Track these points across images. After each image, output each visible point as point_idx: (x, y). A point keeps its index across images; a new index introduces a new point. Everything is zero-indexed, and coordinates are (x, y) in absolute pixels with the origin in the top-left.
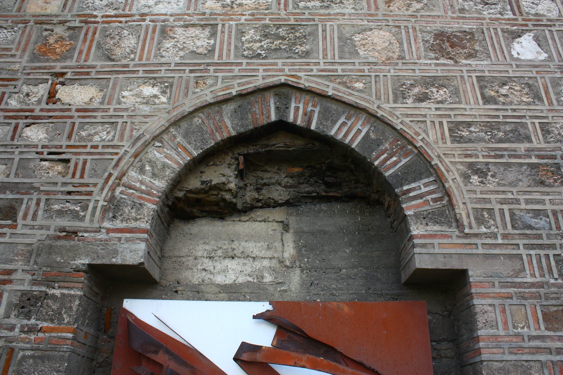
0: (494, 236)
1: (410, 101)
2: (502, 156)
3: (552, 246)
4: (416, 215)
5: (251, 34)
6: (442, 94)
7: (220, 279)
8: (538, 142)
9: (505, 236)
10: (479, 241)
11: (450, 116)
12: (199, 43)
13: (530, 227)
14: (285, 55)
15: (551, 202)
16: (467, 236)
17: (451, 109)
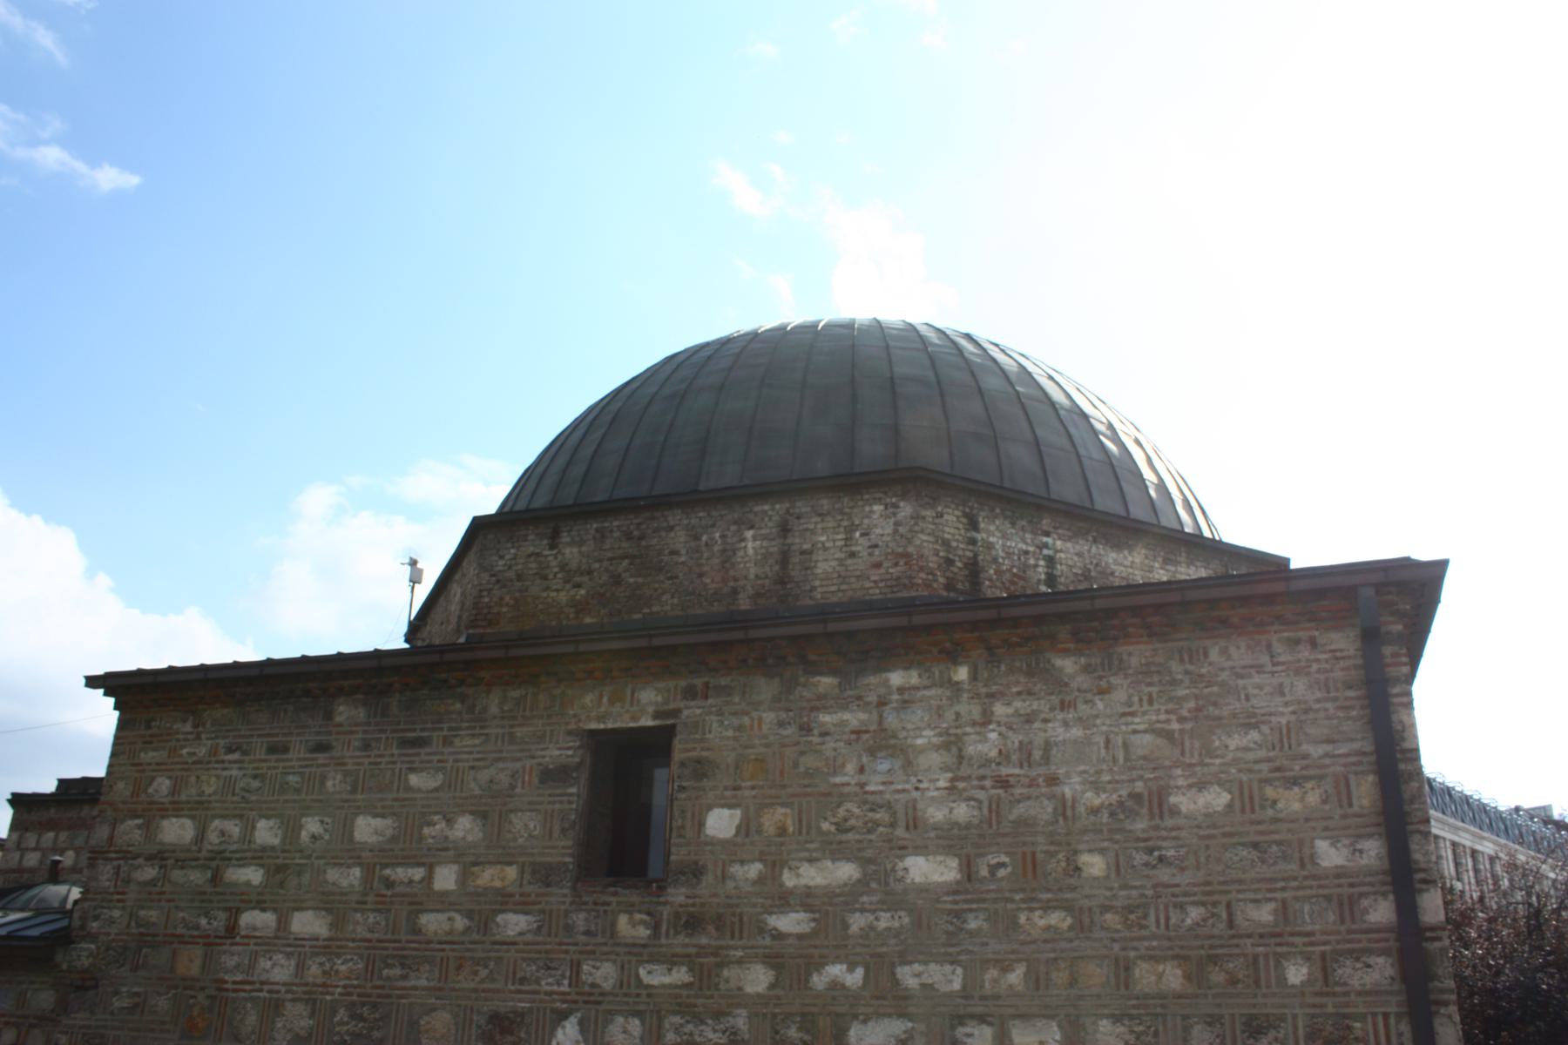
5: (342, 1014)
12: (303, 1023)
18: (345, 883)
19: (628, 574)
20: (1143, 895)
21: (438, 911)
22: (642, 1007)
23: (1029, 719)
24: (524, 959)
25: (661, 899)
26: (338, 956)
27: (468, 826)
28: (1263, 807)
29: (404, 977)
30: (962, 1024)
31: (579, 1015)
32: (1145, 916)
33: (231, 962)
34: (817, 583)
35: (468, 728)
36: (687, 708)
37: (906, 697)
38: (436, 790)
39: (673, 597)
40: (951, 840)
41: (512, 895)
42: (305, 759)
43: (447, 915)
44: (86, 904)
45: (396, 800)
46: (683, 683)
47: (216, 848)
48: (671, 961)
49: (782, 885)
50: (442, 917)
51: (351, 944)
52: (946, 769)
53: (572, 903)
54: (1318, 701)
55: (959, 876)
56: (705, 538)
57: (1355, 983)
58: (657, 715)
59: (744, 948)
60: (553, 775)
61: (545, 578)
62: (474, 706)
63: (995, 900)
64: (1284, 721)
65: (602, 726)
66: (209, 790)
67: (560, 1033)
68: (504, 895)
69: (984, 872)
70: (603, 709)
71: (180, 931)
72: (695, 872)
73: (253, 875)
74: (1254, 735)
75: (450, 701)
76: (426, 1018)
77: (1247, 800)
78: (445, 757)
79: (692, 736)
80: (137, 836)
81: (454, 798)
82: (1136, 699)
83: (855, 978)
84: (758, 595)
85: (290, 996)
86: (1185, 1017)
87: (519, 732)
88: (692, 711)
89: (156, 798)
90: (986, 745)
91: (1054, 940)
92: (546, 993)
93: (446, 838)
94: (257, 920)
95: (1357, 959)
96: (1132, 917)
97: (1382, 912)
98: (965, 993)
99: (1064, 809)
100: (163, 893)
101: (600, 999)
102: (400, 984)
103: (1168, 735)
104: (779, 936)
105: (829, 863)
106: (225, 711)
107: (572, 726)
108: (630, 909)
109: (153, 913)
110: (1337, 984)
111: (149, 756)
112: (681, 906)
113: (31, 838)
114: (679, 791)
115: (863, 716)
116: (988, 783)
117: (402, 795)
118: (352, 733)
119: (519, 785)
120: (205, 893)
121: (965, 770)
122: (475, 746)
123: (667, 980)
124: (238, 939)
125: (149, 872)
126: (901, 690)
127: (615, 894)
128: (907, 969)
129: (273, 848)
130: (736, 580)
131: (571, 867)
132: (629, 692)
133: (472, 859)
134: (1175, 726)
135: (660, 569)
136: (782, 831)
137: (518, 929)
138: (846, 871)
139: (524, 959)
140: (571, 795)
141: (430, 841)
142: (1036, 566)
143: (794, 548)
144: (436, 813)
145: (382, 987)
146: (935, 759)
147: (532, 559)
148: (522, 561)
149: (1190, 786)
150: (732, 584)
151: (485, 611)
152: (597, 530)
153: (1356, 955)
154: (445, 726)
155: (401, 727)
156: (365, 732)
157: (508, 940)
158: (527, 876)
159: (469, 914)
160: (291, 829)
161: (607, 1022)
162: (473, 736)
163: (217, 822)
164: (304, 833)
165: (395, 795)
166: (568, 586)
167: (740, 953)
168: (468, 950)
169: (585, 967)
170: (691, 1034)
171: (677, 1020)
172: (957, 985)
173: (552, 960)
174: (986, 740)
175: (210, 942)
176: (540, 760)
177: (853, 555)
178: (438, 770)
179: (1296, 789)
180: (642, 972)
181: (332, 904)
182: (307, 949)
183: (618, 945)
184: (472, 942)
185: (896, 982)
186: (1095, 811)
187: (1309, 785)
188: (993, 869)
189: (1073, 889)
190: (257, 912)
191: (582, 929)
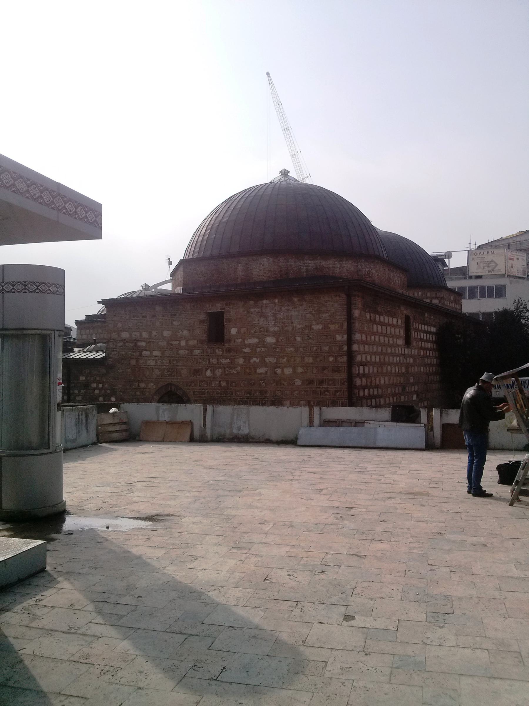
6: (193, 385)
18: (163, 345)
20: (307, 345)
22: (221, 367)
23: (288, 310)
28: (328, 328)
30: (276, 368)
32: (307, 349)
33: (142, 362)
34: (253, 277)
37: (266, 305)
38: (179, 325)
40: (275, 334)
46: (225, 302)
47: (135, 338)
48: (226, 358)
49: (245, 343)
52: (273, 320)
54: (339, 308)
55: (276, 341)
56: (230, 266)
57: (340, 361)
59: (239, 355)
60: (202, 322)
63: (282, 346)
64: (333, 311)
66: (131, 326)
69: (280, 340)
71: (130, 356)
72: (229, 341)
73: (143, 344)
74: (327, 314)
77: (325, 327)
82: (307, 307)
83: (258, 360)
84: (242, 279)
86: (312, 367)
88: (227, 308)
90: (280, 316)
91: (291, 353)
93: (182, 335)
95: (341, 357)
96: (305, 349)
97: (345, 348)
98: (276, 363)
99: (293, 328)
103: (312, 314)
104: (245, 353)
105: (253, 339)
107: (205, 312)
110: (337, 361)
113: (83, 332)
115: (258, 309)
116: (281, 323)
121: (277, 321)
125: (121, 344)
126: (266, 304)
128: (266, 358)
129: (147, 338)
130: (237, 276)
134: (314, 312)
136: (245, 333)
138: (256, 340)
142: (303, 268)
143: (249, 268)
146: (271, 318)
149: (316, 324)
150: (237, 277)
153: (341, 356)
158: (198, 342)
159: (188, 350)
163: (134, 333)
164: (153, 335)
167: (238, 356)
170: (230, 371)
171: (228, 369)
172: (275, 361)
174: (280, 314)
177: (261, 270)
178: (179, 321)
179: (334, 325)
185: (265, 361)
186: (299, 329)
187: (336, 324)
188: (281, 340)
189: (295, 343)
191: (210, 352)
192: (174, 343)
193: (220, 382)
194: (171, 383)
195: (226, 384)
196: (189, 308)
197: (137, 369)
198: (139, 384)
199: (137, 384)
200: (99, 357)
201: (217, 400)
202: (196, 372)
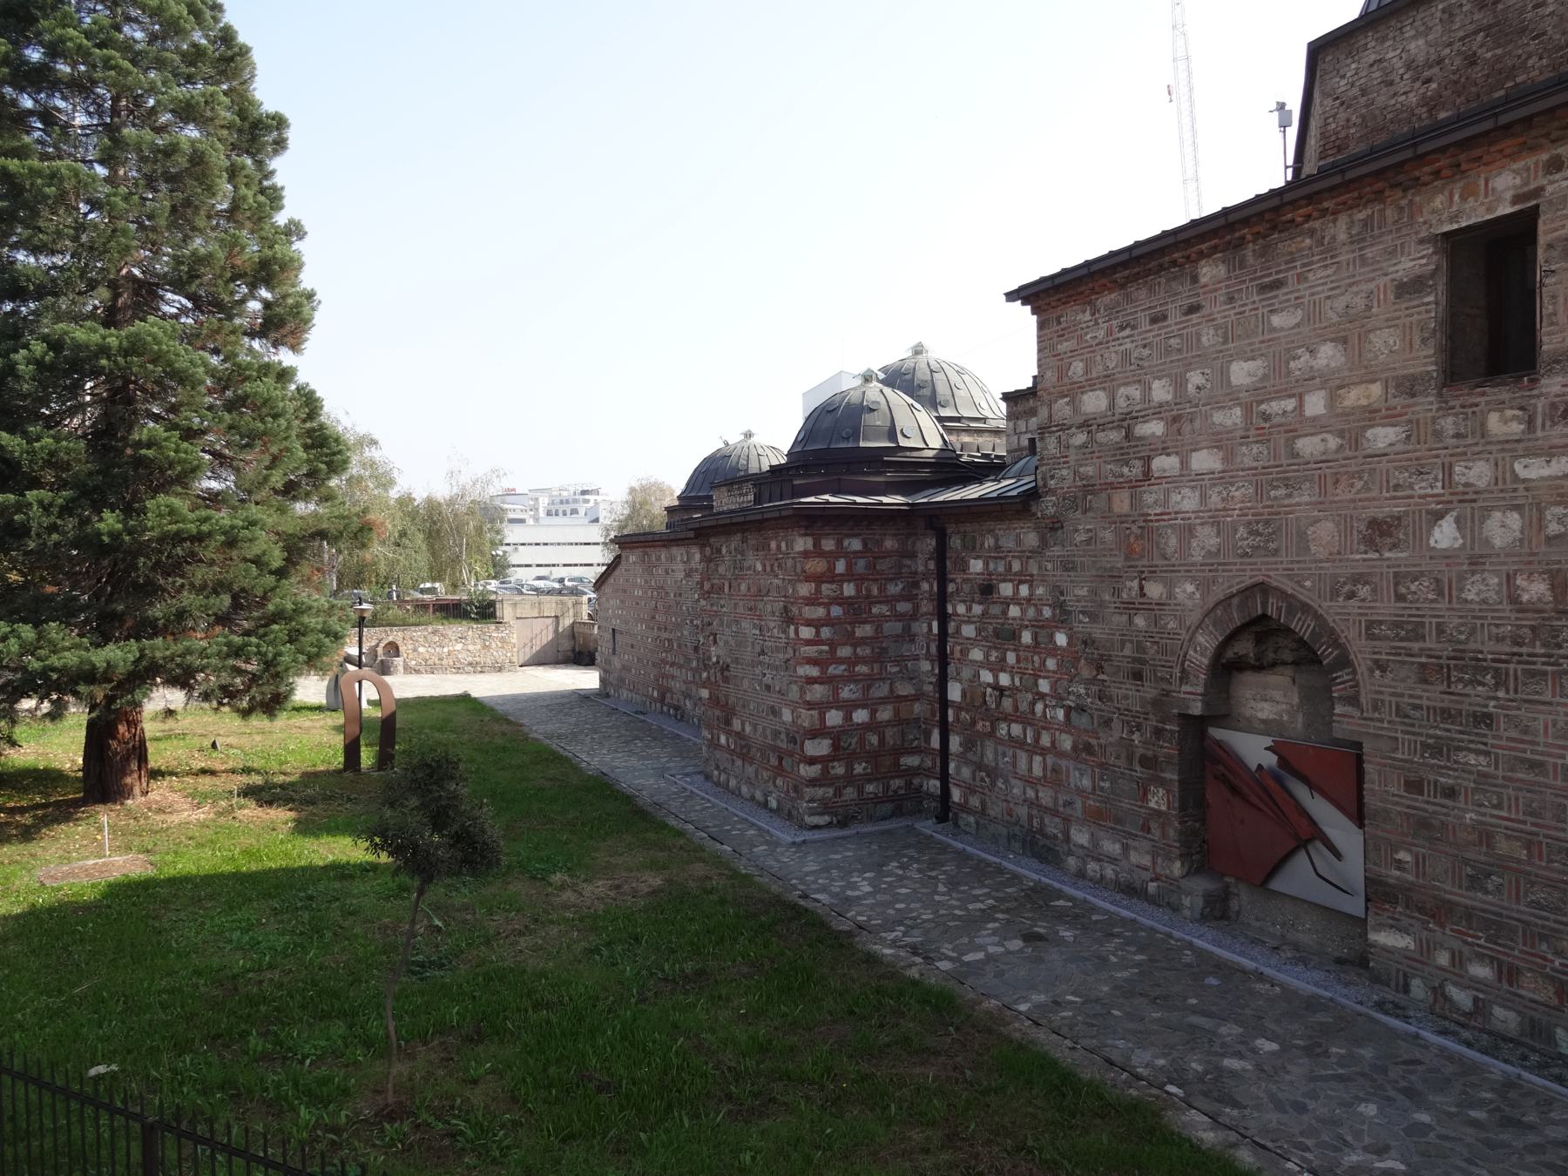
0: (1381, 721)
1: (1341, 599)
2: (1400, 654)
3: (1420, 734)
4: (1340, 698)
6: (1364, 591)
7: (1260, 715)
8: (1430, 643)
9: (1389, 722)
10: (1372, 724)
11: (1366, 615)
13: (1407, 716)
14: (1263, 552)
15: (1428, 699)
16: (1365, 719)
17: (1370, 608)
18: (1229, 422)
19: (1484, 49)
21: (1312, 435)
24: (1396, 468)
25: (1535, 392)
26: (1232, 484)
27: (1330, 353)
29: (1289, 496)
31: (1455, 514)
35: (1319, 261)
36: (1551, 183)
38: (1298, 325)
39: (1541, 58)
41: (1380, 411)
42: (1182, 322)
43: (1320, 437)
44: (1044, 468)
45: (1263, 342)
46: (1545, 157)
47: (1125, 411)
50: (1316, 439)
51: (1241, 473)
53: (1438, 410)
58: (1516, 199)
60: (1408, 288)
61: (1391, 83)
62: (1323, 237)
65: (1455, 226)
67: (1437, 531)
68: (1371, 412)
70: (1454, 208)
71: (1110, 479)
73: (1155, 428)
75: (1299, 239)
76: (1312, 529)
78: (1302, 293)
79: (1559, 213)
80: (1068, 411)
81: (1315, 329)
85: (1198, 521)
87: (1369, 253)
89: (1076, 379)
92: (1420, 497)
93: (1312, 367)
94: (1165, 464)
100: (1093, 452)
101: (1474, 497)
102: (1286, 502)
106: (1113, 296)
108: (1500, 406)
109: (1089, 468)
111: (1064, 347)
112: (1557, 396)
113: (1022, 425)
114: (1547, 277)
117: (1267, 337)
118: (1216, 290)
119: (1375, 304)
120: (1122, 448)
122: (1328, 276)
123: (1546, 472)
124: (1153, 481)
125: (1080, 438)
127: (1483, 394)
131: (1435, 375)
132: (1482, 182)
133: (1337, 382)
135: (1523, 31)
137: (1388, 441)
139: (1396, 468)
140: (1428, 303)
141: (1298, 373)
144: (1299, 347)
145: (1272, 506)
147: (1375, 66)
148: (1364, 74)
151: (1333, 138)
152: (1444, 11)
154: (1298, 264)
155: (1258, 274)
156: (1227, 287)
157: (1378, 452)
158: (1392, 391)
159: (1341, 434)
160: (1179, 383)
161: (1483, 520)
162: (1326, 266)
163: (1122, 390)
164: (1190, 386)
165: (1261, 338)
166: (1417, 85)
168: (1343, 466)
169: (1457, 469)
173: (1422, 466)
175: (1133, 486)
176: (1394, 276)
178: (1297, 306)
180: (1518, 467)
181: (1220, 441)
182: (1206, 482)
183: (1490, 443)
184: (1345, 459)
190: (1164, 457)
191: (1451, 433)
192: (1275, 407)
193: (1510, 578)
194: (1262, 583)
195: (1553, 588)
196: (1342, 237)
197: (1134, 528)
198: (1141, 588)
199: (1135, 584)
200: (1014, 493)
201: (1497, 670)
202: (1380, 531)
